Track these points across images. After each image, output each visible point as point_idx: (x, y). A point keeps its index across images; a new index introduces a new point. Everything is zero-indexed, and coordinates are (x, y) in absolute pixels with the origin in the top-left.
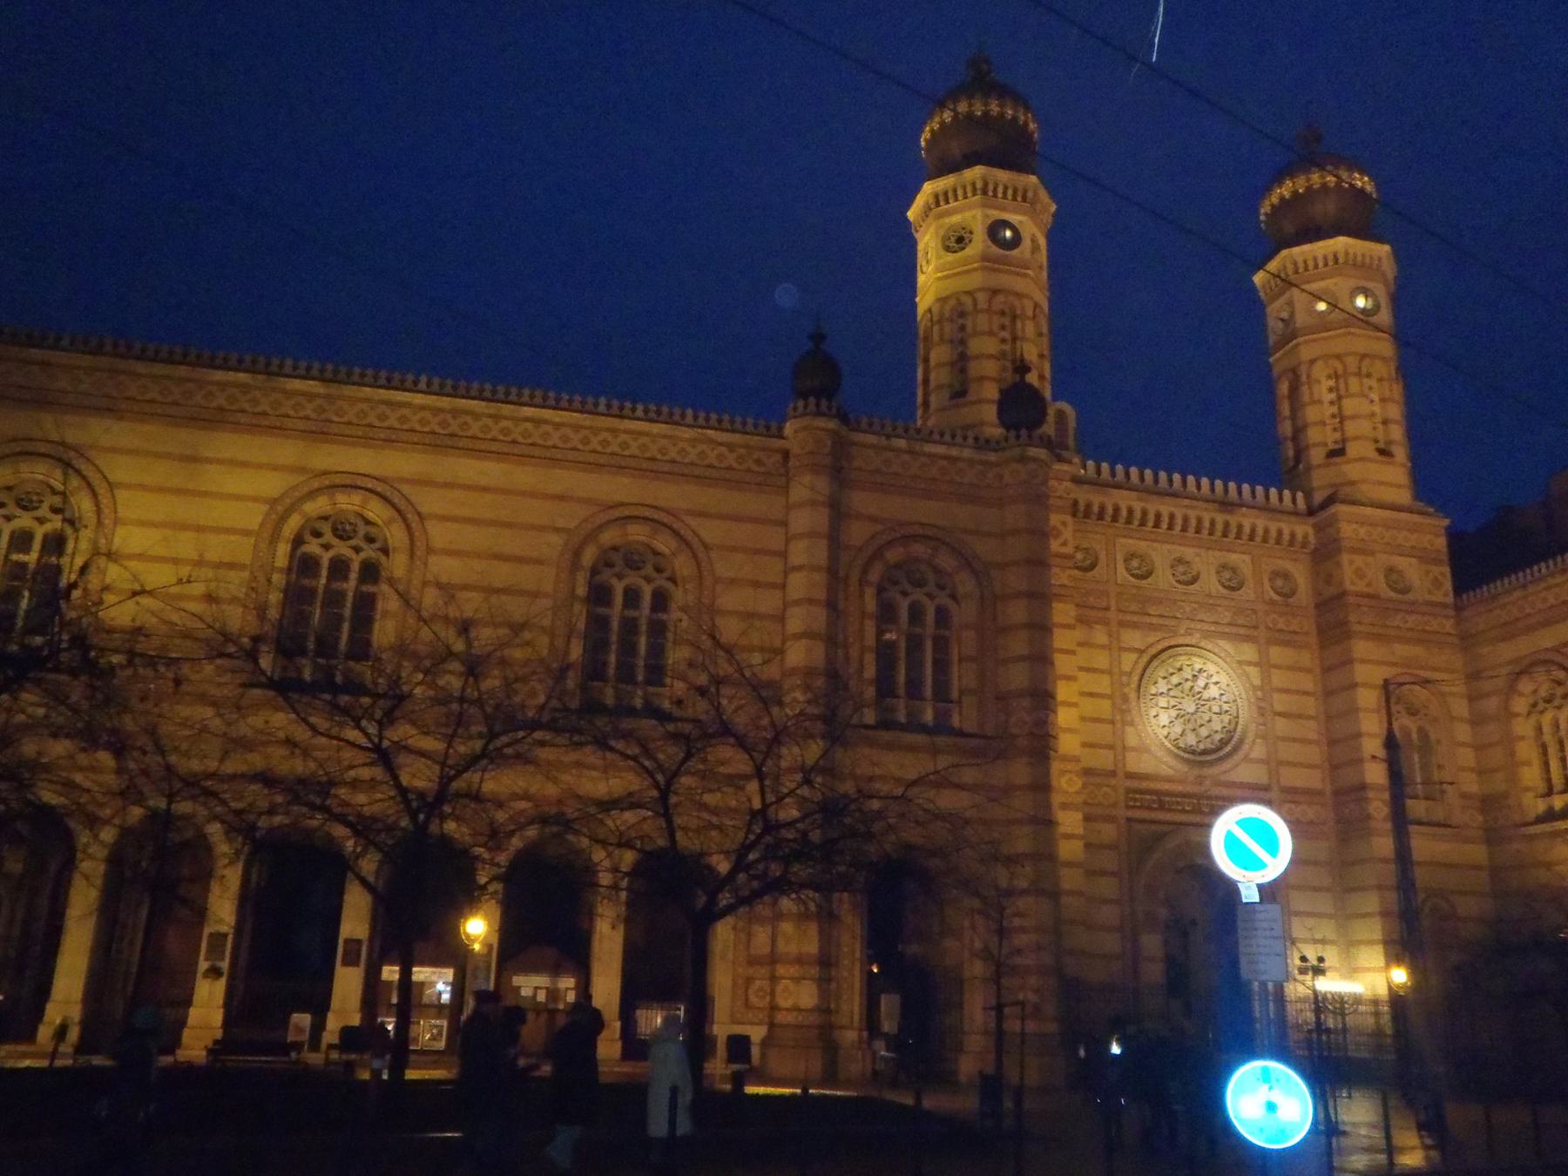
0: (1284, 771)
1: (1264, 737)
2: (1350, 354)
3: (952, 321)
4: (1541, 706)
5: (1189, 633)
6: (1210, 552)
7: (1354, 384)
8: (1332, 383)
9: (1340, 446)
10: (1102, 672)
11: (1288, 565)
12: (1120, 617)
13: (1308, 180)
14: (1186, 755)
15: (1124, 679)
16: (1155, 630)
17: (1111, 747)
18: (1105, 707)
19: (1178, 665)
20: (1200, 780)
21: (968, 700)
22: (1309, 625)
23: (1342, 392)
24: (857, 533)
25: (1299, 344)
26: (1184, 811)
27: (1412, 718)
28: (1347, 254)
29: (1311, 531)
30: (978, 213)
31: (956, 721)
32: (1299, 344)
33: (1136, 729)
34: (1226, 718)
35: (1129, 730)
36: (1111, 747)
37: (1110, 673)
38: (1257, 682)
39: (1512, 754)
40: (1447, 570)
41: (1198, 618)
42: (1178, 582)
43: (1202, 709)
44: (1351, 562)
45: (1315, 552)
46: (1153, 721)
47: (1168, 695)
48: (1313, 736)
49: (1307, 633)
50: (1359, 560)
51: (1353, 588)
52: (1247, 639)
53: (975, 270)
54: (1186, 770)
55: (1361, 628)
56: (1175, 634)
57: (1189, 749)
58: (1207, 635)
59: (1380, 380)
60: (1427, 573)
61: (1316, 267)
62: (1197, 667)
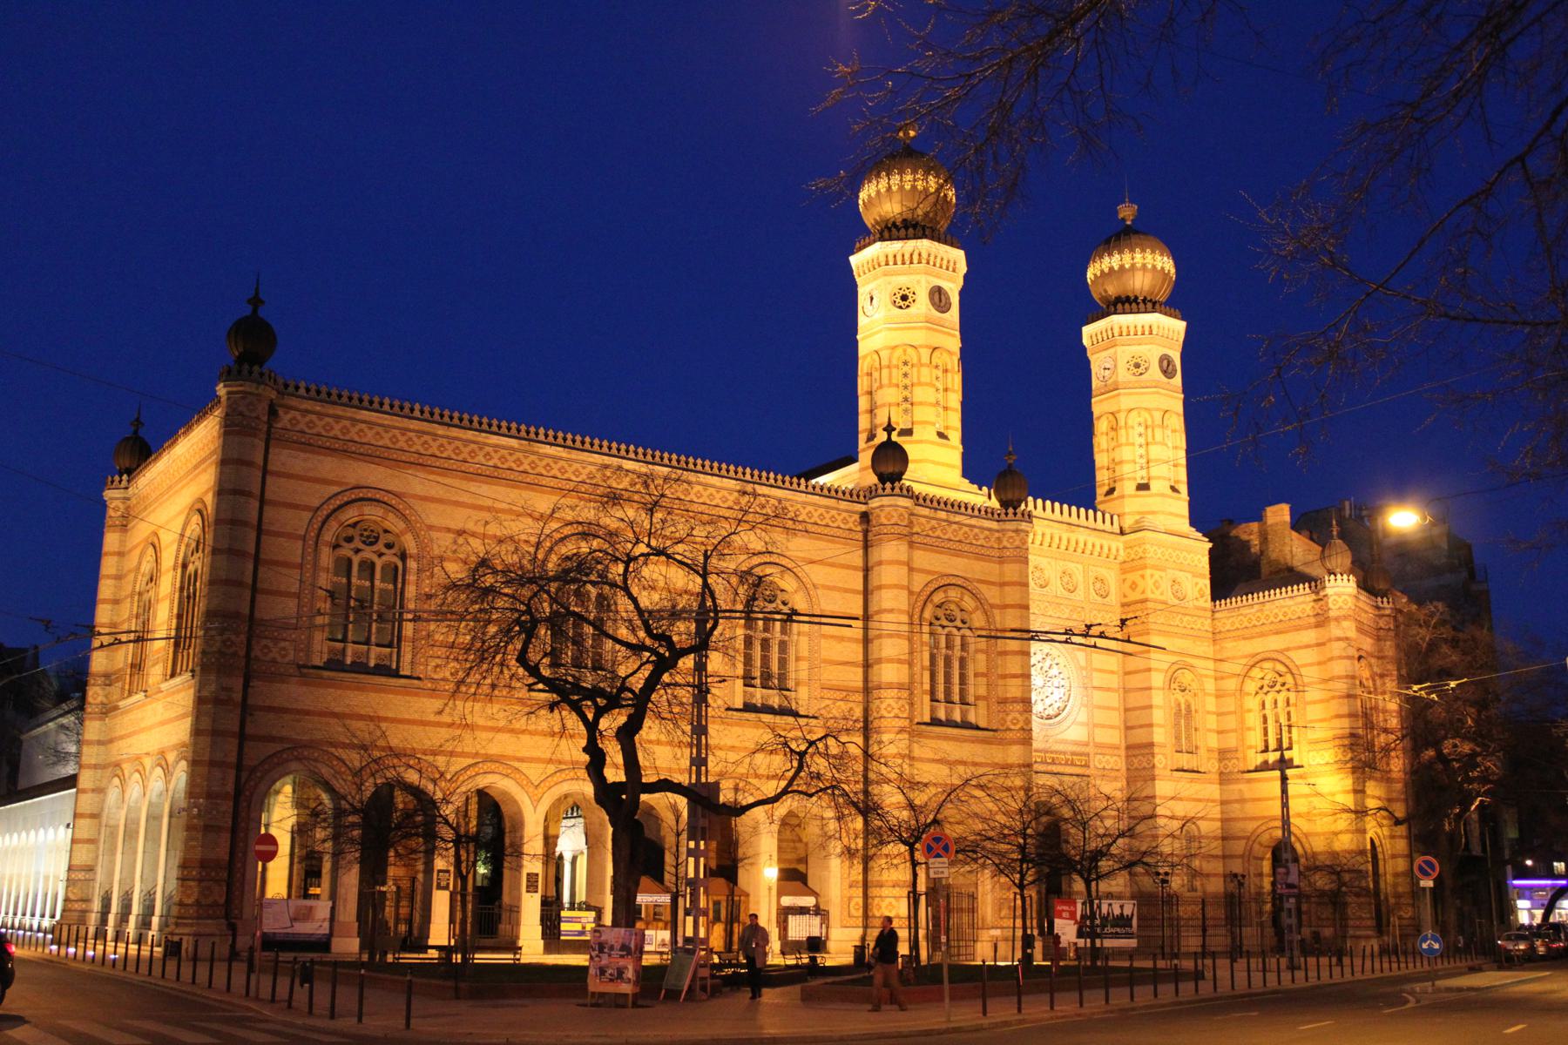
0: (1098, 731)
1: (1086, 706)
2: (1158, 409)
3: (897, 367)
4: (1266, 689)
21: (982, 704)
23: (1150, 440)
24: (919, 581)
29: (1121, 546)
30: (923, 278)
31: (972, 718)
32: (1118, 395)
38: (1083, 663)
39: (1242, 721)
44: (1152, 576)
48: (1115, 704)
50: (1157, 574)
53: (921, 328)
62: (1046, 651)
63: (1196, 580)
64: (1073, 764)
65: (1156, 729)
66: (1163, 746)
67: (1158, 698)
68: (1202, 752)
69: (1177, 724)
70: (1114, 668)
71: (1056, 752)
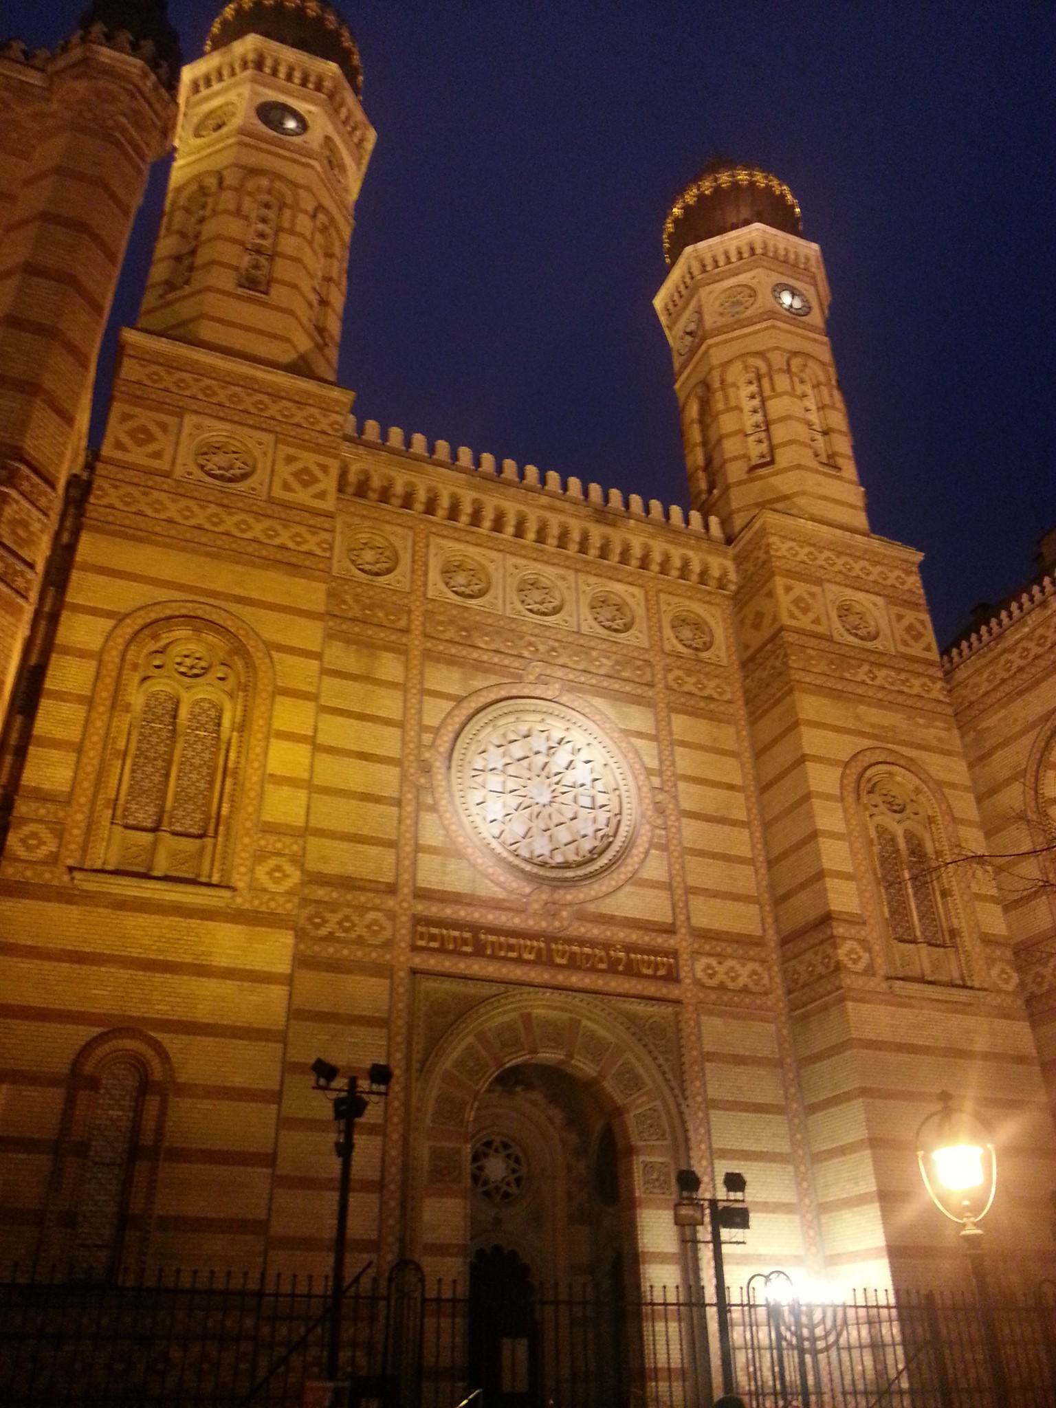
0: (696, 902)
1: (664, 848)
2: (778, 348)
5: (542, 680)
6: (581, 577)
7: (782, 382)
8: (754, 388)
9: (768, 459)
10: (388, 722)
11: (699, 608)
12: (429, 645)
13: (716, 180)
14: (528, 868)
15: (427, 738)
16: (487, 671)
17: (392, 844)
18: (387, 779)
19: (523, 728)
20: (552, 910)
22: (733, 691)
25: (710, 347)
26: (519, 961)
27: (897, 816)
28: (765, 247)
29: (730, 565)
32: (706, 352)
33: (441, 818)
34: (602, 816)
35: (428, 818)
36: (392, 844)
37: (400, 725)
38: (653, 764)
40: (926, 618)
41: (560, 661)
42: (531, 611)
43: (561, 799)
44: (788, 589)
45: (735, 597)
46: (474, 810)
47: (503, 772)
49: (729, 702)
50: (800, 589)
51: (793, 623)
52: (637, 700)
54: (528, 890)
55: (809, 679)
56: (519, 679)
57: (537, 860)
58: (573, 687)
59: (816, 386)
60: (900, 617)
61: (728, 261)
62: (557, 735)
63: (895, 610)
64: (631, 971)
65: (830, 883)
66: (855, 921)
67: (829, 818)
68: (969, 941)
69: (890, 882)
70: (737, 780)
71: (582, 942)
